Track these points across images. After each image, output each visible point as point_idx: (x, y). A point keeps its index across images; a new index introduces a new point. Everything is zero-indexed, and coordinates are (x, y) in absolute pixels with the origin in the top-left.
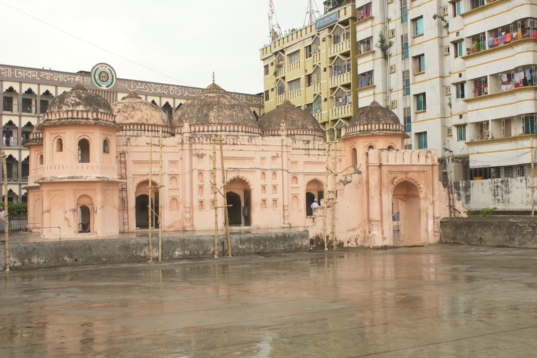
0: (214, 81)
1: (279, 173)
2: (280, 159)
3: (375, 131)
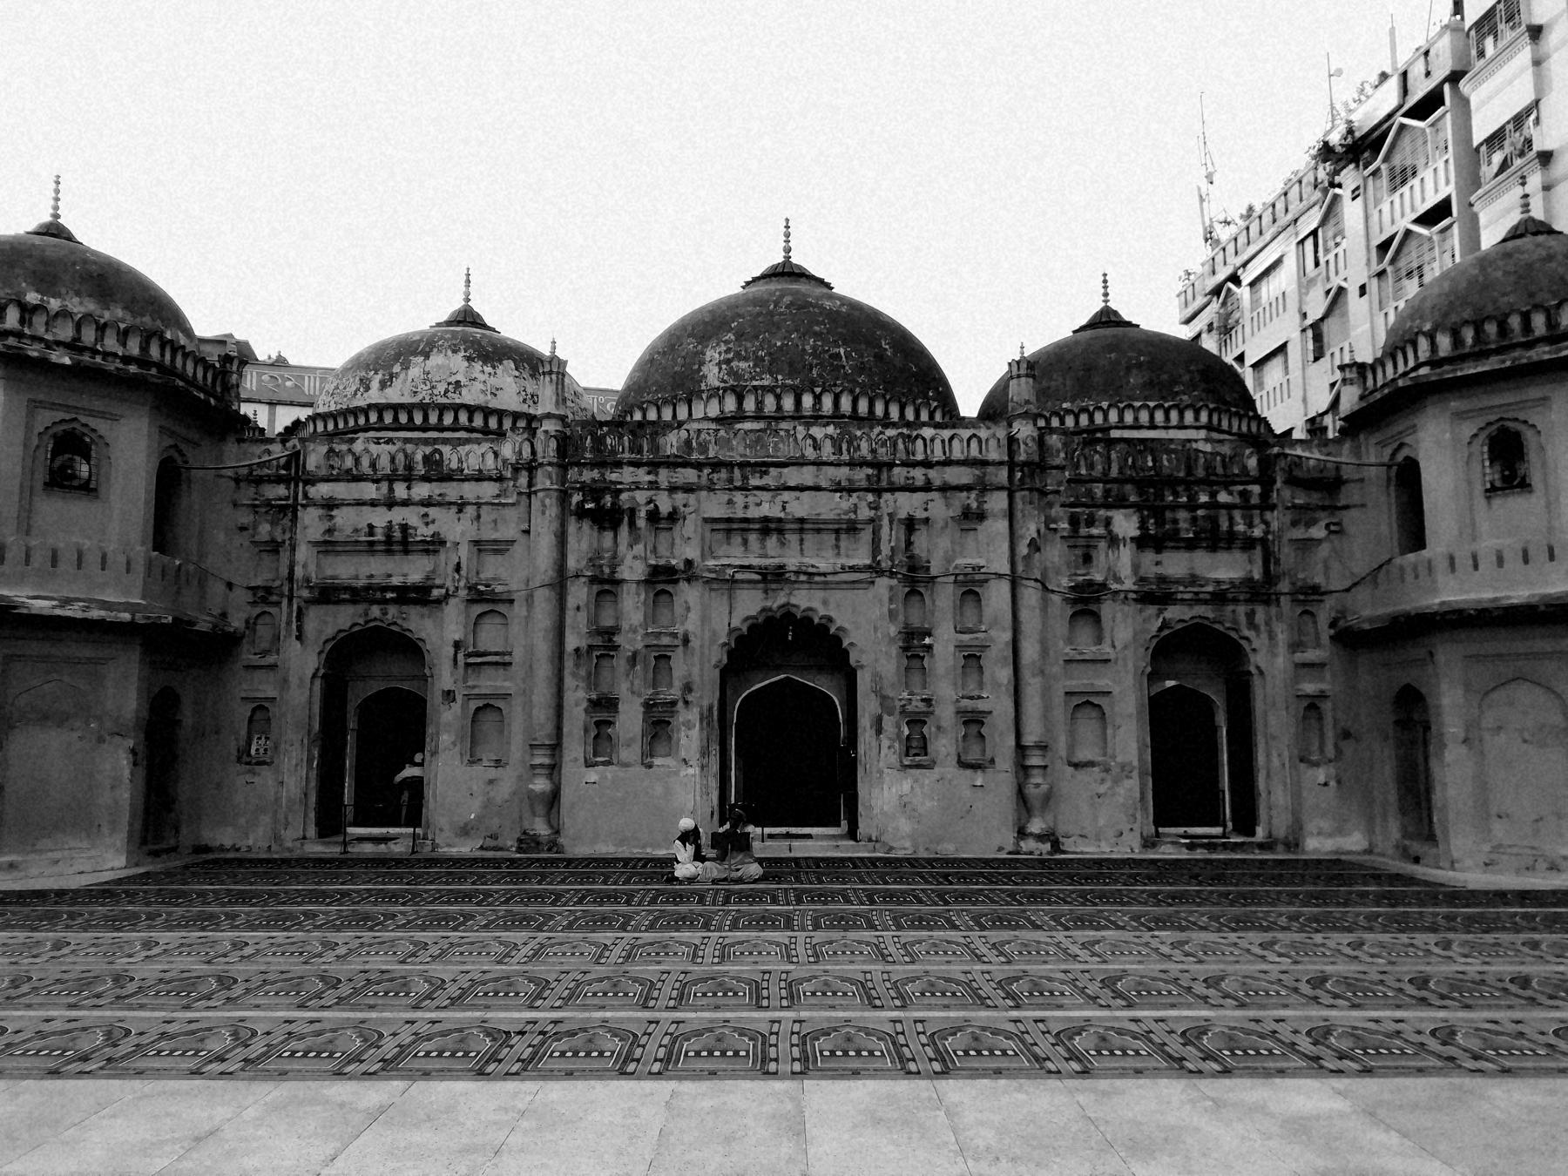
0: (788, 250)
1: (997, 596)
2: (1002, 525)
3: (1529, 345)
